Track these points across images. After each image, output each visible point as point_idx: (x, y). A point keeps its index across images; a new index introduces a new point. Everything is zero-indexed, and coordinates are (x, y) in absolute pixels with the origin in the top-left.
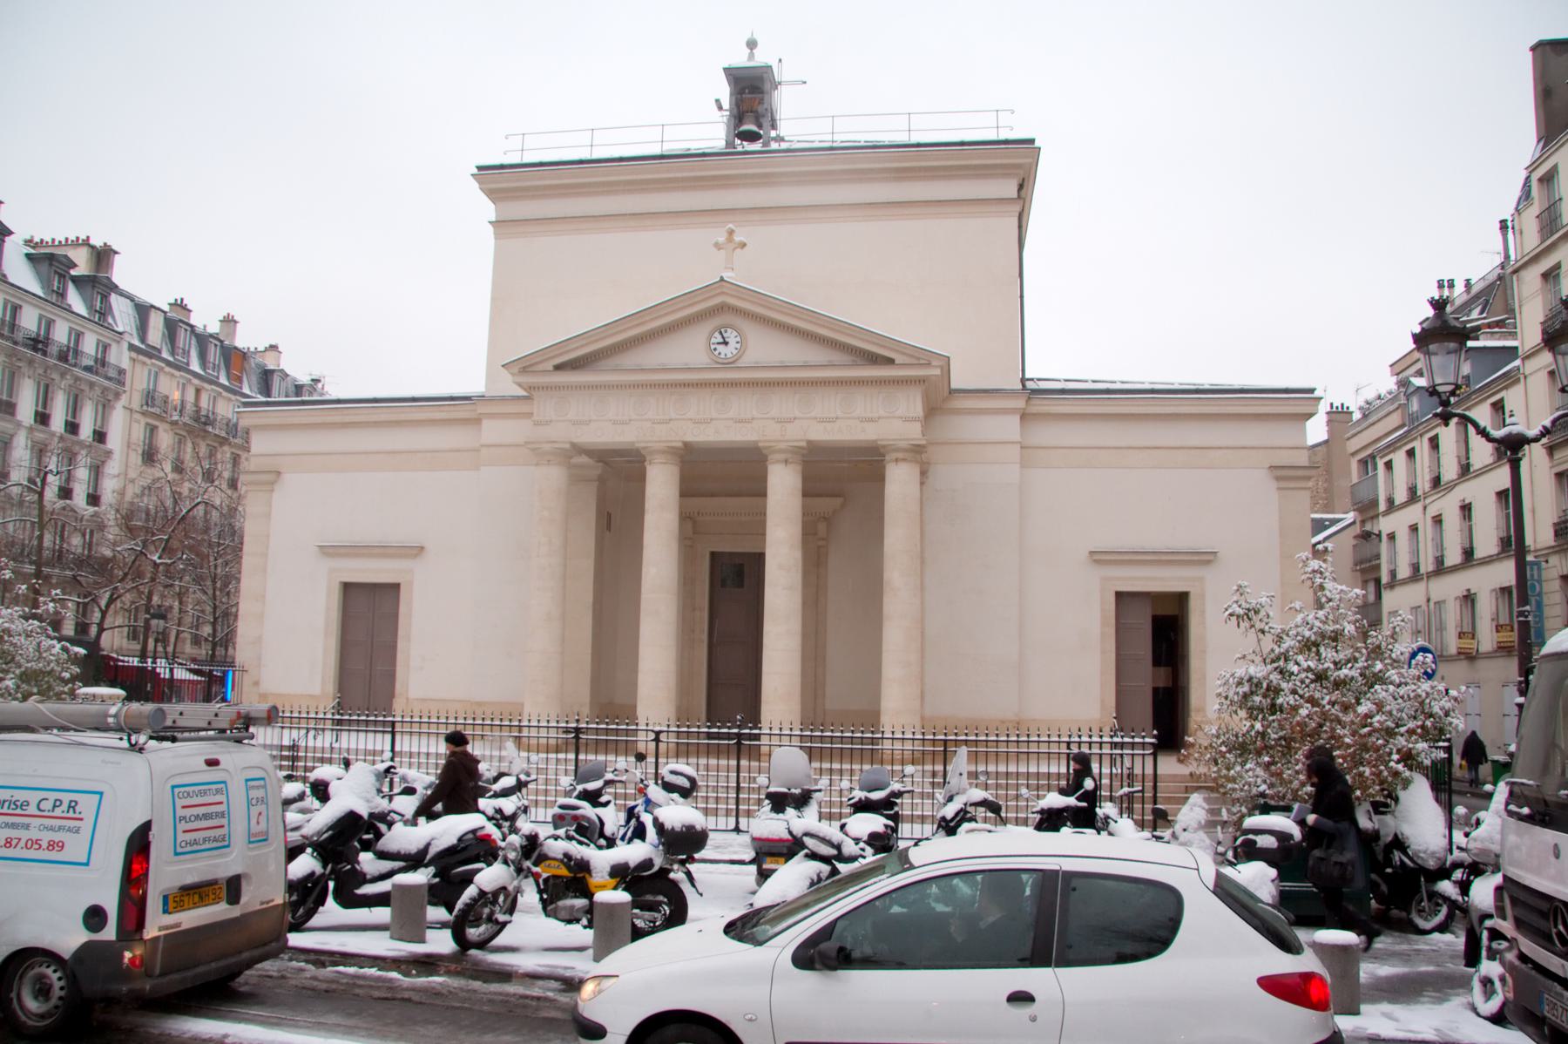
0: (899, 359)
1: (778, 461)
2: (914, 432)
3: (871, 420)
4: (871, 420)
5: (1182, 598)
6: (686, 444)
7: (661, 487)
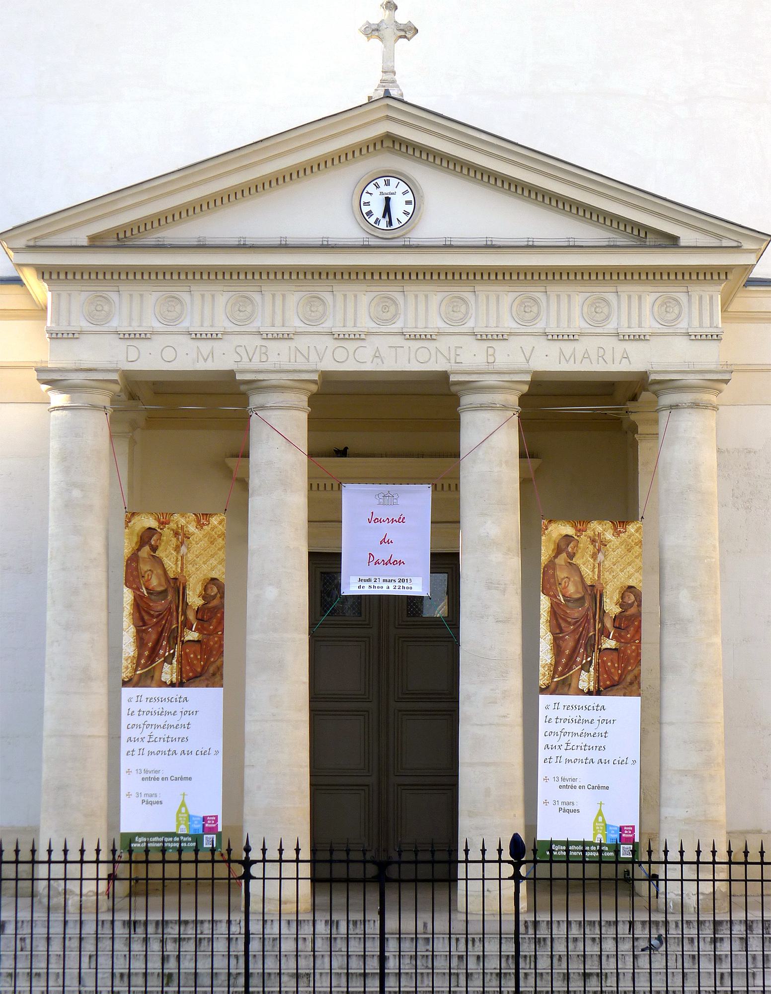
0: (687, 237)
1: (482, 407)
2: (707, 356)
3: (639, 338)
4: (639, 338)
7: (279, 449)
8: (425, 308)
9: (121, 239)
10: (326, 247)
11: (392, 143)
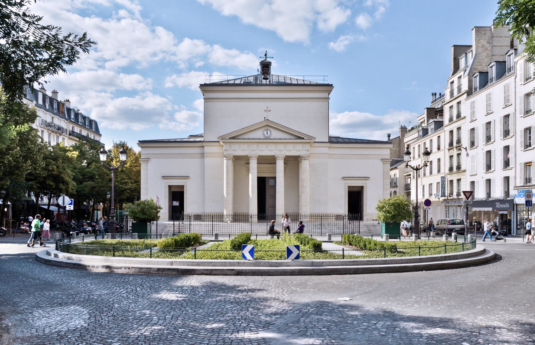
0: (305, 138)
2: (308, 153)
5: (362, 187)
6: (259, 156)
7: (253, 164)
8: (272, 147)
9: (233, 138)
10: (259, 139)
11: (267, 126)
